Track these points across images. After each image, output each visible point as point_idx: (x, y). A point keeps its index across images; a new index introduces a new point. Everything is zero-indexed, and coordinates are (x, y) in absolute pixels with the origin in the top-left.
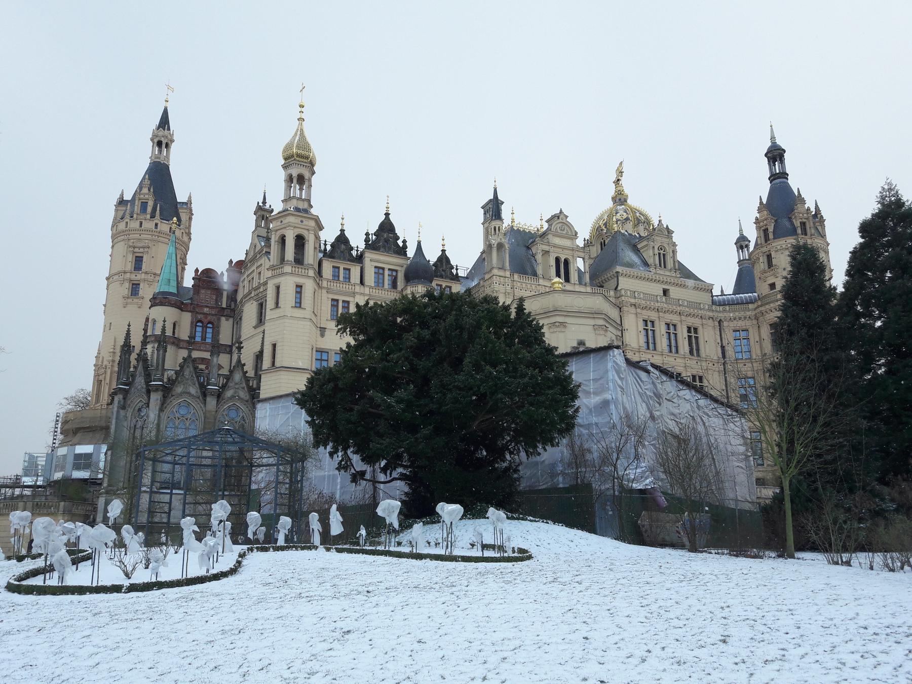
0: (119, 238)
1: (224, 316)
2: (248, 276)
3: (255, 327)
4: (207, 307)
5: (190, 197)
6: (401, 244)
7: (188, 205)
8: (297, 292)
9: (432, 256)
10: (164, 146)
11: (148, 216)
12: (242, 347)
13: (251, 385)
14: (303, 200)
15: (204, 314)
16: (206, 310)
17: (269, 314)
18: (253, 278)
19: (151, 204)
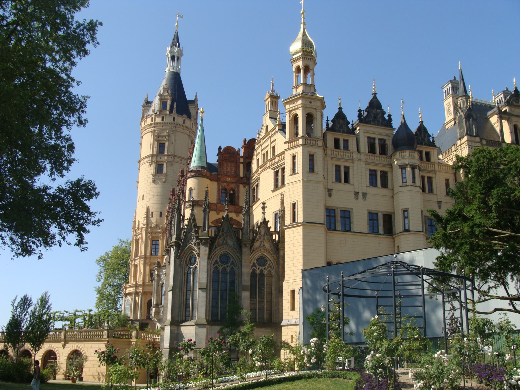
0: (147, 130)
1: (242, 184)
2: (262, 150)
3: (273, 191)
4: (229, 176)
5: (196, 96)
6: (387, 118)
7: (194, 102)
8: (310, 160)
9: (413, 128)
10: (176, 59)
11: (168, 113)
12: (266, 207)
13: (274, 238)
14: (310, 86)
15: (226, 182)
16: (229, 179)
17: (288, 179)
18: (267, 152)
19: (169, 102)
